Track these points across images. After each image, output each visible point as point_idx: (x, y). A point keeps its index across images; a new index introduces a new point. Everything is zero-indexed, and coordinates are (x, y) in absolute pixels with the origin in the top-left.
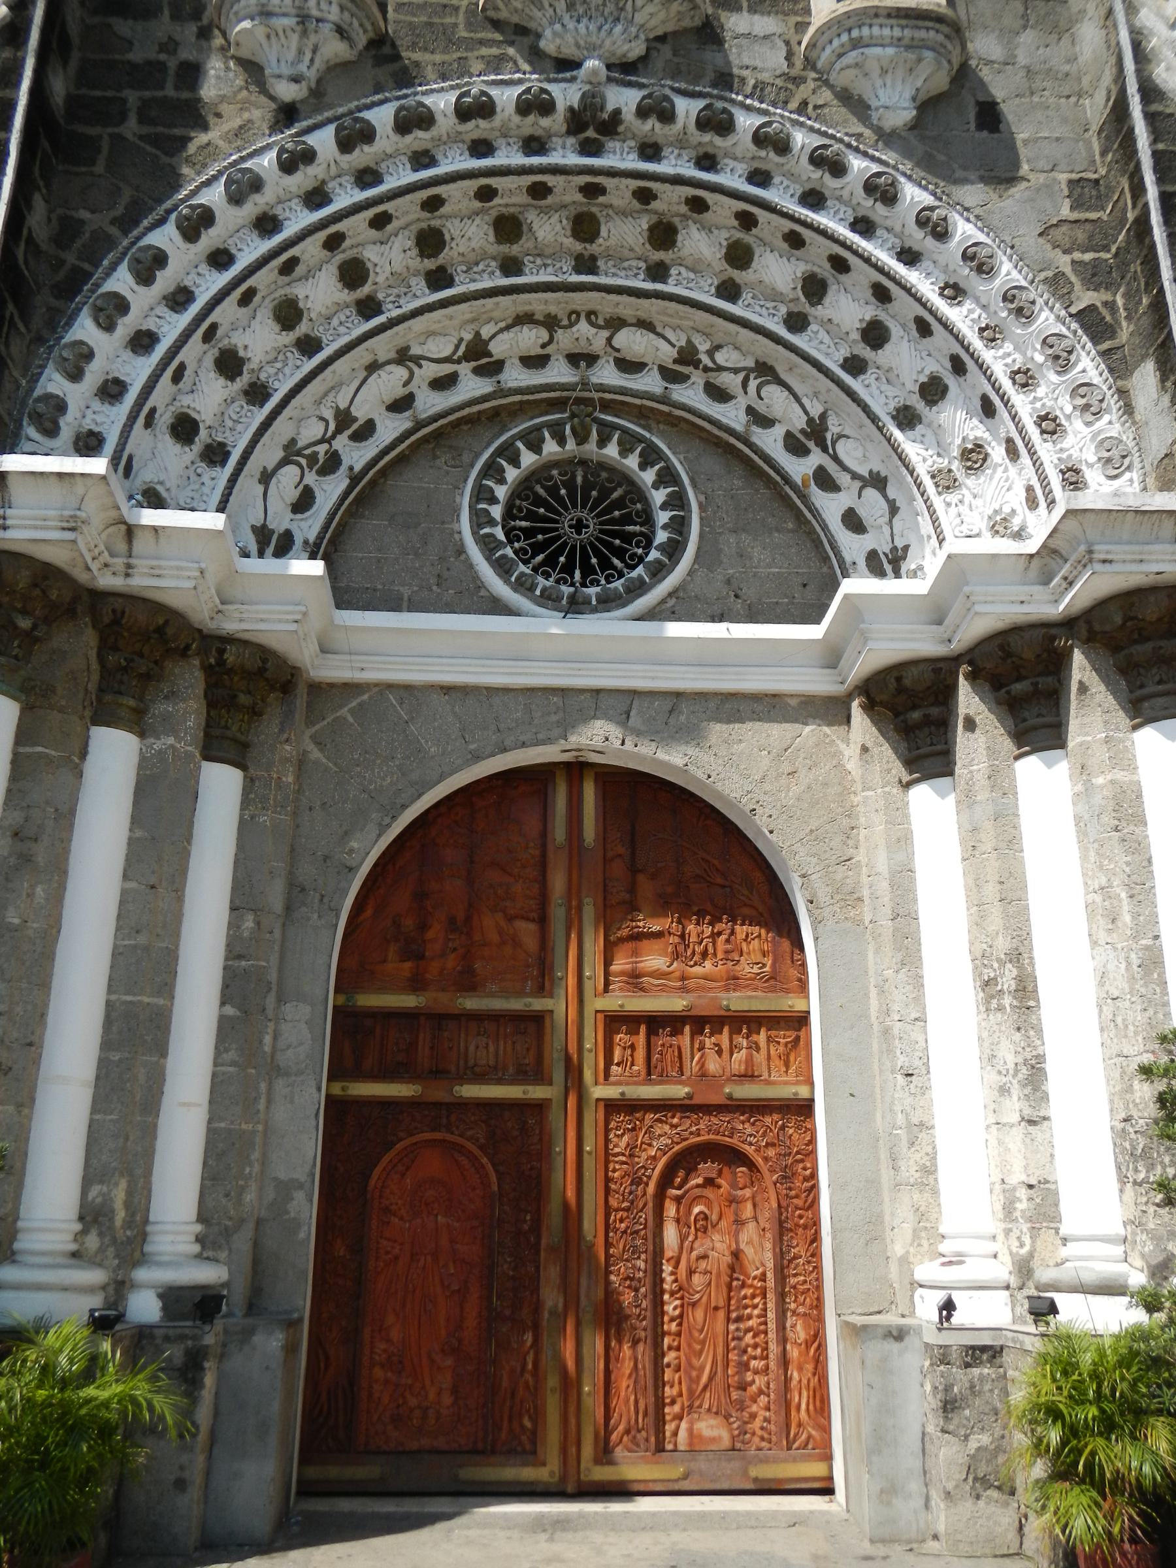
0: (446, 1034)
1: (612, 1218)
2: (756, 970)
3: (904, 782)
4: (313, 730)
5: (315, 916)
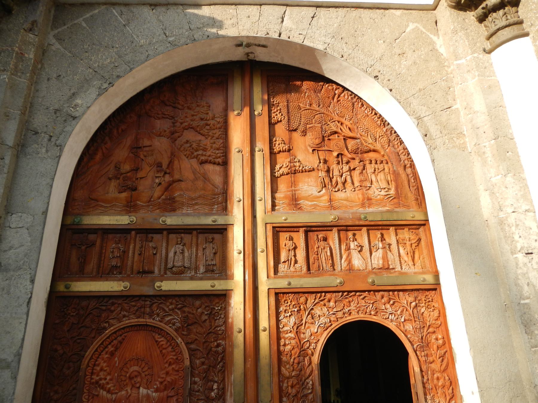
0: (151, 244)
1: (285, 385)
2: (383, 193)
3: (487, 49)
4: (56, 31)
5: (44, 150)
